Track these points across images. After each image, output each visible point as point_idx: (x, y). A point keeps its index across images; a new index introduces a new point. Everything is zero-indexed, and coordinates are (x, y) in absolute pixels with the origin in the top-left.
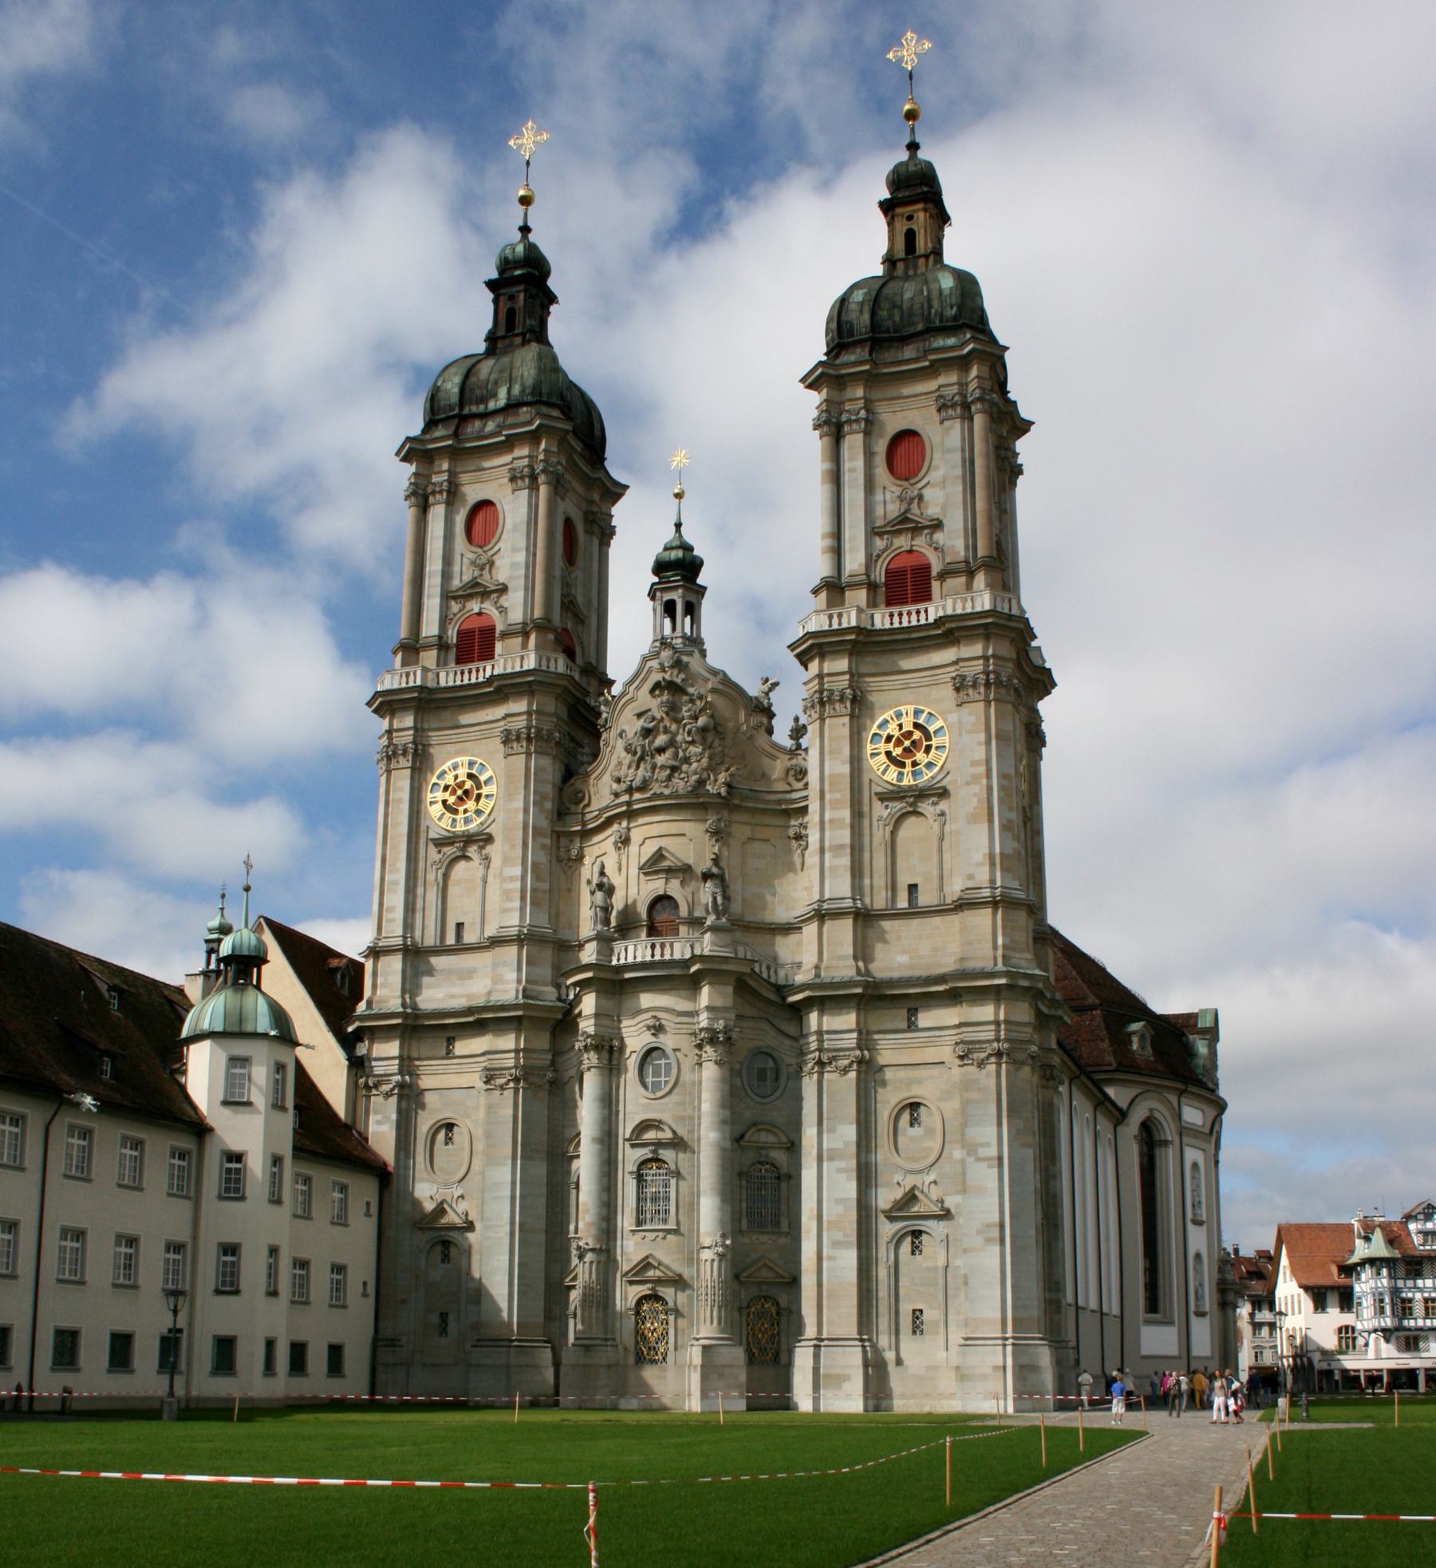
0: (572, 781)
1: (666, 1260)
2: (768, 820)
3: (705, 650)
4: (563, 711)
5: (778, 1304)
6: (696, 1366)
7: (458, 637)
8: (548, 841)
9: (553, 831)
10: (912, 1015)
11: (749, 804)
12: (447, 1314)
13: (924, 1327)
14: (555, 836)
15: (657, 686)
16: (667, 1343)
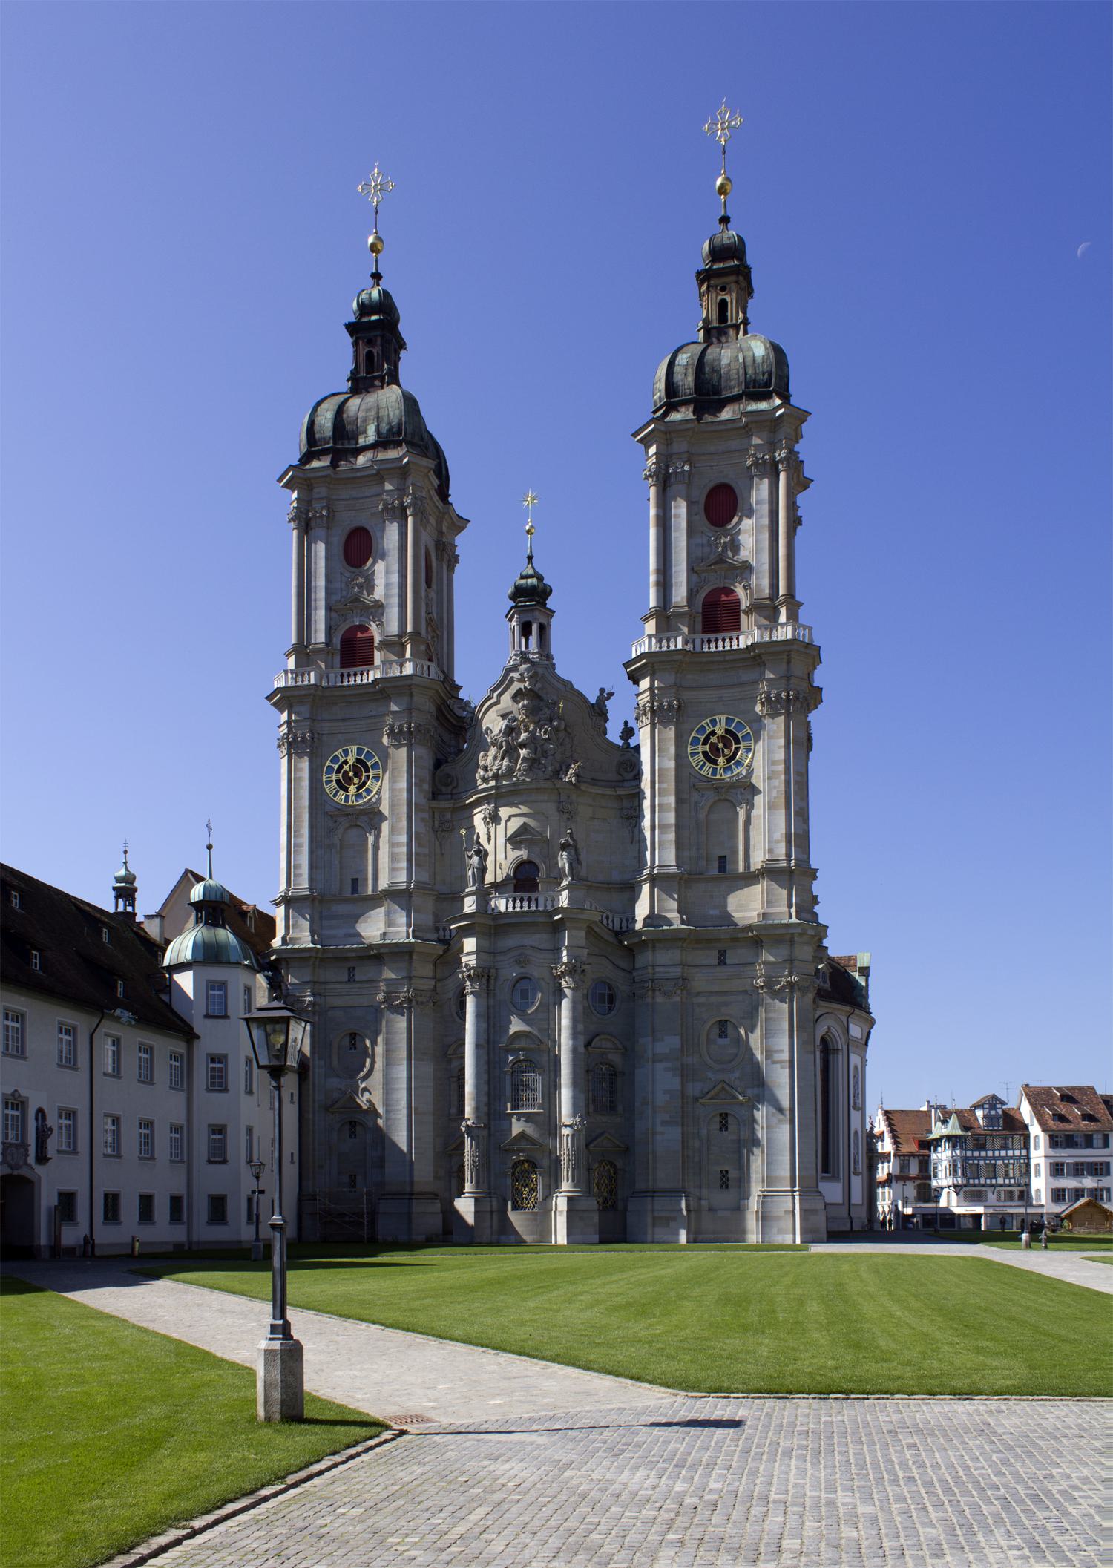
0: (442, 768)
3: (554, 664)
4: (433, 709)
6: (561, 1212)
7: (341, 645)
8: (426, 816)
10: (722, 955)
11: (592, 791)
13: (730, 1183)
15: (519, 693)
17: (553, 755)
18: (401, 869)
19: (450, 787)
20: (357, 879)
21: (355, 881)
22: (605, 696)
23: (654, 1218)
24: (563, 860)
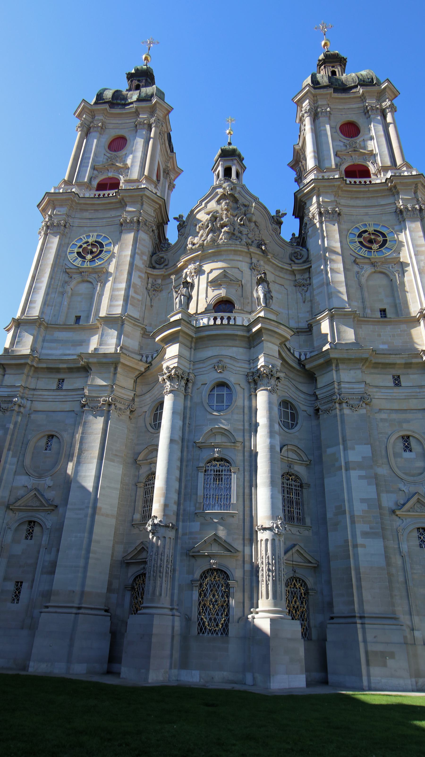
2: (281, 275)
5: (305, 584)
9: (146, 272)
11: (275, 262)
12: (22, 582)
16: (227, 615)
17: (247, 235)
18: (118, 306)
21: (78, 318)
23: (367, 653)
24: (260, 292)
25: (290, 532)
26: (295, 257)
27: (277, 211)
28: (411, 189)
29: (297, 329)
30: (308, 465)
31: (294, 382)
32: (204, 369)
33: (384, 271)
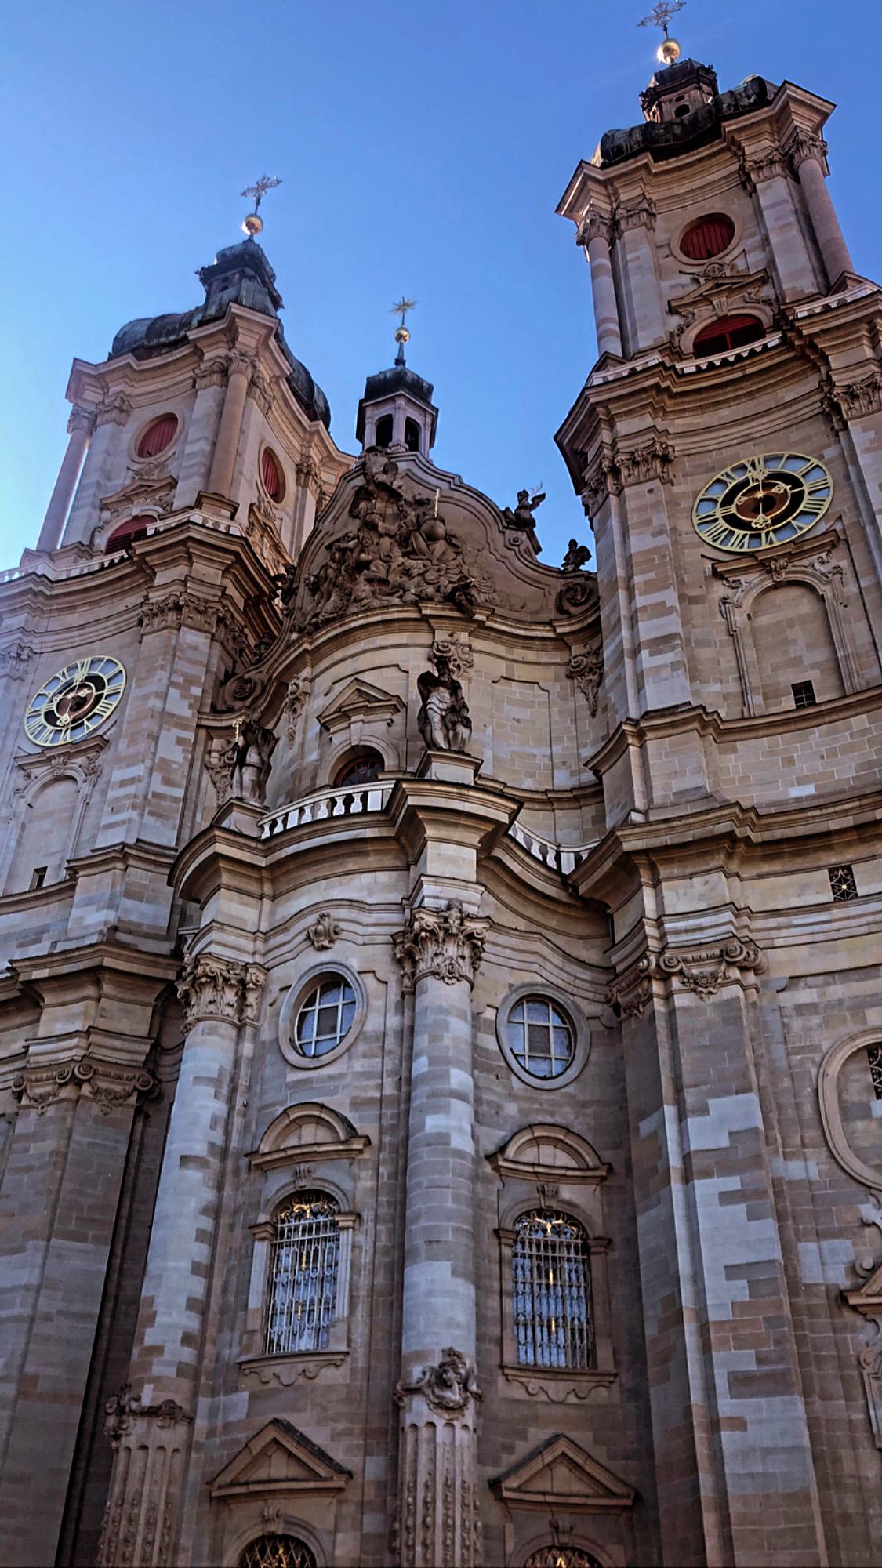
1: (319, 1437)
8: (190, 736)
9: (199, 726)
14: (203, 733)
19: (250, 700)
20: (45, 869)
22: (528, 502)
25: (543, 1397)
26: (569, 600)
27: (519, 494)
28: (859, 339)
29: (571, 790)
30: (603, 1179)
31: (560, 941)
32: (286, 948)
33: (799, 577)
